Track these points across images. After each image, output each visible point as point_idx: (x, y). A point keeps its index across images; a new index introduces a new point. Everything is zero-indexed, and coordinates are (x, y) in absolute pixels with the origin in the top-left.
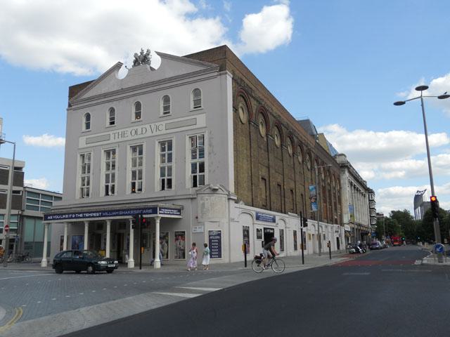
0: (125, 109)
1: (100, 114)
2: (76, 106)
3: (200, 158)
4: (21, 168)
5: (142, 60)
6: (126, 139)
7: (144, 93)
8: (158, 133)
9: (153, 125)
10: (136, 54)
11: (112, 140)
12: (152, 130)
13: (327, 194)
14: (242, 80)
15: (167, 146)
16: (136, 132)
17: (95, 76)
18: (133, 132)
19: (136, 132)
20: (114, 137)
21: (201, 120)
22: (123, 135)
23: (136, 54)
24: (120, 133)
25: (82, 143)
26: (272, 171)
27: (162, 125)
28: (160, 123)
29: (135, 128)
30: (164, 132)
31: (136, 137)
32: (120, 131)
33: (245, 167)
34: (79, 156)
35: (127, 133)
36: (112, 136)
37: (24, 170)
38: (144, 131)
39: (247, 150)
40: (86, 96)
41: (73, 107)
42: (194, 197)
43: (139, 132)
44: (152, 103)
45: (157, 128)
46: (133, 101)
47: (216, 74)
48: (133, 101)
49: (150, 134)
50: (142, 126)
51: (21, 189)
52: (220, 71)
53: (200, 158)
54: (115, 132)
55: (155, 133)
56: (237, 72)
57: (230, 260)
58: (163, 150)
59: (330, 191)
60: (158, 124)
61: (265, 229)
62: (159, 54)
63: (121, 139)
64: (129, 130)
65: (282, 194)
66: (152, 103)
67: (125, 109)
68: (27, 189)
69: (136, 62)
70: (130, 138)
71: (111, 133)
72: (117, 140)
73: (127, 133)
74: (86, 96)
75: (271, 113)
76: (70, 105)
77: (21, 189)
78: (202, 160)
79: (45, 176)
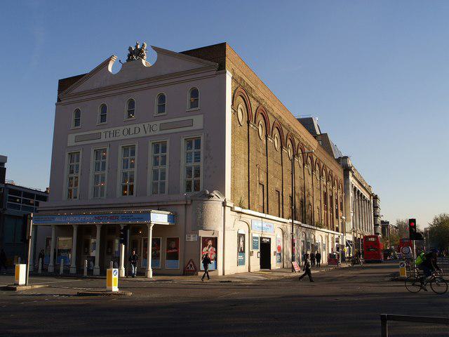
0: (117, 106)
1: (91, 110)
2: (67, 101)
3: (195, 162)
4: (3, 164)
5: (136, 53)
6: (117, 138)
7: (137, 90)
8: (152, 133)
10: (130, 49)
11: (103, 139)
12: (147, 128)
13: (329, 200)
14: (241, 79)
15: (160, 147)
16: (129, 131)
17: (88, 71)
18: (126, 132)
20: (105, 135)
21: (198, 121)
22: (115, 133)
23: (130, 49)
25: (71, 140)
26: (271, 176)
27: (157, 124)
28: (154, 123)
29: (128, 127)
30: (158, 132)
31: (128, 137)
32: (112, 130)
33: (243, 172)
34: (67, 156)
35: (119, 132)
36: (103, 135)
37: (6, 165)
39: (245, 154)
40: (76, 91)
41: (63, 102)
42: (189, 203)
43: (132, 131)
45: (151, 128)
46: (126, 98)
47: (215, 72)
48: (126, 98)
49: (144, 135)
50: (135, 126)
51: (3, 186)
52: (219, 70)
53: (195, 162)
54: (106, 130)
55: (148, 134)
56: (237, 71)
57: (224, 274)
58: (157, 151)
59: (331, 197)
60: (152, 124)
61: (261, 238)
62: (155, 49)
64: (122, 128)
65: (281, 202)
67: (117, 106)
68: (9, 186)
70: (122, 137)
73: (119, 132)
74: (76, 91)
75: (271, 114)
76: (59, 100)
77: (3, 186)
78: (197, 164)
79: (31, 172)
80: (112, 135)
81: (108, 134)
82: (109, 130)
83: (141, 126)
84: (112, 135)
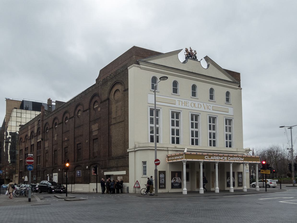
8: (208, 111)
9: (205, 104)
10: (187, 50)
16: (194, 105)
18: (193, 105)
19: (194, 105)
22: (186, 104)
24: (183, 102)
31: (194, 108)
32: (183, 101)
36: (177, 103)
38: (200, 106)
43: (197, 106)
44: (203, 88)
55: (206, 110)
60: (208, 105)
63: (183, 107)
64: (190, 102)
66: (203, 88)
67: (185, 85)
69: (187, 58)
70: (190, 108)
71: (177, 100)
72: (180, 106)
80: (183, 104)
81: (181, 104)
82: (181, 100)
83: (202, 104)
84: (183, 104)
